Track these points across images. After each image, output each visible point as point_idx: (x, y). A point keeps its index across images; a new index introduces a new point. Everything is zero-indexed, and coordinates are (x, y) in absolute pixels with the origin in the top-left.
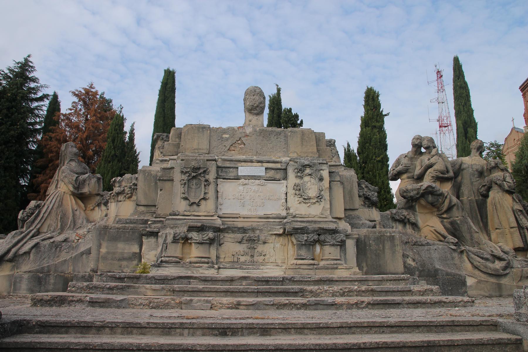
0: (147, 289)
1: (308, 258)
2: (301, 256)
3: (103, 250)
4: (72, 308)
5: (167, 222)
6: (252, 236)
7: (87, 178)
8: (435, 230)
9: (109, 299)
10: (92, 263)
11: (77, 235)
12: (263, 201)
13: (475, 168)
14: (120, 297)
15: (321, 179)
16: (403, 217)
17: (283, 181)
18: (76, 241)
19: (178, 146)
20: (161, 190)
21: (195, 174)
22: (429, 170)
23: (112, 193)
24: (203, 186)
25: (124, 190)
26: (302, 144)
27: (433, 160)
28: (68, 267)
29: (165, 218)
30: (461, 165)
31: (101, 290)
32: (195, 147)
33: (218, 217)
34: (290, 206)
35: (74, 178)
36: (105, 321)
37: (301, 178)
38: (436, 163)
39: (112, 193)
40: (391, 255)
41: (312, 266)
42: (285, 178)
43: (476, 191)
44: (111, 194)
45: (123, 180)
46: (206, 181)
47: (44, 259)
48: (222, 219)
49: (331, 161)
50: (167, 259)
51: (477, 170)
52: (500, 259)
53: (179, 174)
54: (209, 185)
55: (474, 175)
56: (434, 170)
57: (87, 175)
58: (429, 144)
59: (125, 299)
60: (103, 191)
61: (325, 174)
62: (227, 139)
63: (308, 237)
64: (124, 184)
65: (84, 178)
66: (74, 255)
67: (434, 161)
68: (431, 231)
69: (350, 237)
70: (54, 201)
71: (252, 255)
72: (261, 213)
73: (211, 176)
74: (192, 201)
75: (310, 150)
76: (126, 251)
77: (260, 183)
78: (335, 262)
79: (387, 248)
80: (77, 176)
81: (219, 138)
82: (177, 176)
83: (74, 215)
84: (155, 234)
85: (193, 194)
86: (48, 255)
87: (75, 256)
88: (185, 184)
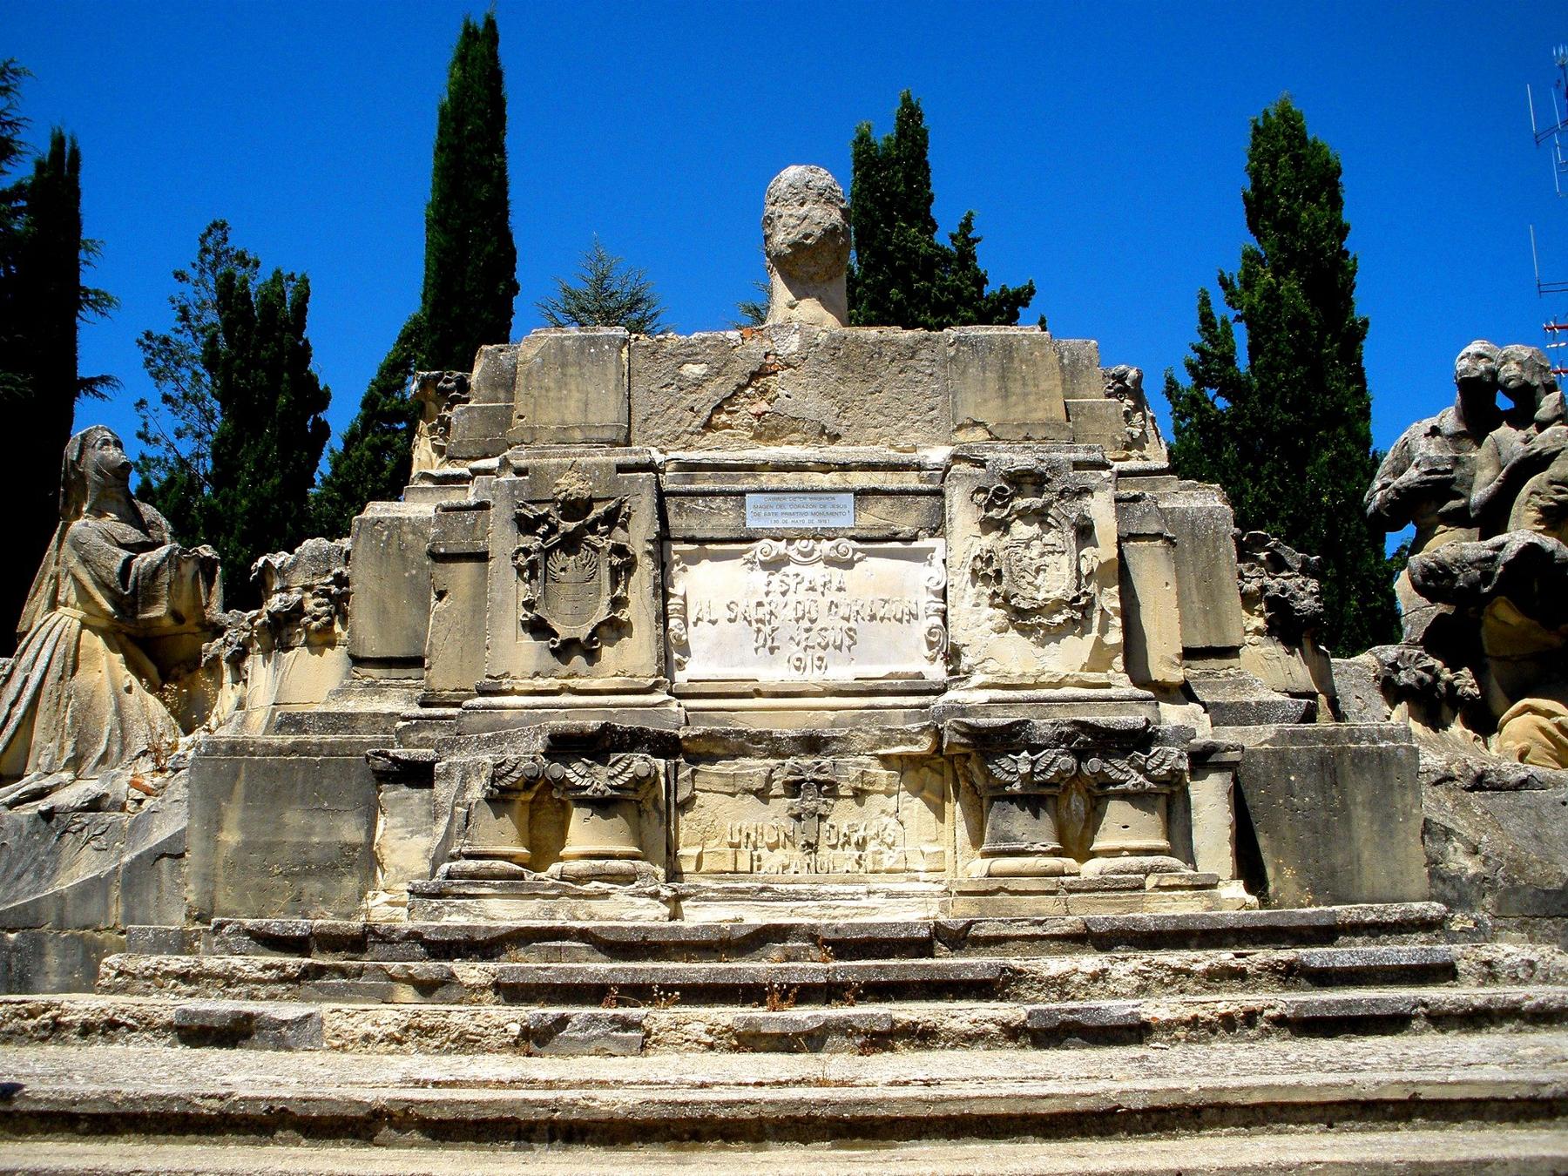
0: (393, 978)
1: (1037, 847)
2: (1006, 838)
3: (231, 837)
4: (116, 1048)
5: (466, 719)
6: (809, 768)
7: (163, 560)
8: (1560, 726)
9: (249, 1017)
10: (191, 887)
11: (133, 784)
12: (852, 624)
14: (290, 1011)
15: (1085, 532)
16: (1428, 677)
17: (925, 543)
18: (131, 806)
19: (502, 419)
20: (441, 595)
21: (571, 526)
22: (1532, 483)
23: (259, 616)
24: (605, 573)
25: (300, 603)
26: (1005, 393)
28: (107, 906)
29: (458, 705)
31: (220, 983)
32: (572, 415)
33: (670, 693)
34: (960, 642)
35: (117, 565)
36: (230, 1095)
37: (1003, 526)
38: (1556, 453)
39: (259, 616)
40: (1375, 828)
41: (1054, 879)
42: (937, 527)
44: (251, 621)
45: (294, 565)
46: (620, 550)
47: (19, 877)
48: (684, 702)
49: (1127, 458)
50: (472, 865)
53: (511, 531)
54: (630, 567)
56: (1551, 483)
57: (162, 551)
58: (1526, 376)
59: (310, 1016)
60: (226, 610)
61: (1101, 509)
62: (698, 384)
63: (1034, 763)
64: (299, 579)
65: (151, 564)
66: (126, 859)
67: (1549, 443)
68: (1542, 730)
69: (1213, 759)
70: (46, 653)
71: (809, 845)
72: (843, 672)
73: (639, 534)
74: (564, 631)
75: (1039, 415)
76: (316, 839)
77: (833, 554)
78: (1148, 861)
79: (1359, 799)
80: (124, 554)
81: (667, 380)
82: (502, 540)
83: (119, 711)
84: (418, 775)
85: (565, 606)
86: (35, 859)
87: (131, 866)
88: (533, 566)
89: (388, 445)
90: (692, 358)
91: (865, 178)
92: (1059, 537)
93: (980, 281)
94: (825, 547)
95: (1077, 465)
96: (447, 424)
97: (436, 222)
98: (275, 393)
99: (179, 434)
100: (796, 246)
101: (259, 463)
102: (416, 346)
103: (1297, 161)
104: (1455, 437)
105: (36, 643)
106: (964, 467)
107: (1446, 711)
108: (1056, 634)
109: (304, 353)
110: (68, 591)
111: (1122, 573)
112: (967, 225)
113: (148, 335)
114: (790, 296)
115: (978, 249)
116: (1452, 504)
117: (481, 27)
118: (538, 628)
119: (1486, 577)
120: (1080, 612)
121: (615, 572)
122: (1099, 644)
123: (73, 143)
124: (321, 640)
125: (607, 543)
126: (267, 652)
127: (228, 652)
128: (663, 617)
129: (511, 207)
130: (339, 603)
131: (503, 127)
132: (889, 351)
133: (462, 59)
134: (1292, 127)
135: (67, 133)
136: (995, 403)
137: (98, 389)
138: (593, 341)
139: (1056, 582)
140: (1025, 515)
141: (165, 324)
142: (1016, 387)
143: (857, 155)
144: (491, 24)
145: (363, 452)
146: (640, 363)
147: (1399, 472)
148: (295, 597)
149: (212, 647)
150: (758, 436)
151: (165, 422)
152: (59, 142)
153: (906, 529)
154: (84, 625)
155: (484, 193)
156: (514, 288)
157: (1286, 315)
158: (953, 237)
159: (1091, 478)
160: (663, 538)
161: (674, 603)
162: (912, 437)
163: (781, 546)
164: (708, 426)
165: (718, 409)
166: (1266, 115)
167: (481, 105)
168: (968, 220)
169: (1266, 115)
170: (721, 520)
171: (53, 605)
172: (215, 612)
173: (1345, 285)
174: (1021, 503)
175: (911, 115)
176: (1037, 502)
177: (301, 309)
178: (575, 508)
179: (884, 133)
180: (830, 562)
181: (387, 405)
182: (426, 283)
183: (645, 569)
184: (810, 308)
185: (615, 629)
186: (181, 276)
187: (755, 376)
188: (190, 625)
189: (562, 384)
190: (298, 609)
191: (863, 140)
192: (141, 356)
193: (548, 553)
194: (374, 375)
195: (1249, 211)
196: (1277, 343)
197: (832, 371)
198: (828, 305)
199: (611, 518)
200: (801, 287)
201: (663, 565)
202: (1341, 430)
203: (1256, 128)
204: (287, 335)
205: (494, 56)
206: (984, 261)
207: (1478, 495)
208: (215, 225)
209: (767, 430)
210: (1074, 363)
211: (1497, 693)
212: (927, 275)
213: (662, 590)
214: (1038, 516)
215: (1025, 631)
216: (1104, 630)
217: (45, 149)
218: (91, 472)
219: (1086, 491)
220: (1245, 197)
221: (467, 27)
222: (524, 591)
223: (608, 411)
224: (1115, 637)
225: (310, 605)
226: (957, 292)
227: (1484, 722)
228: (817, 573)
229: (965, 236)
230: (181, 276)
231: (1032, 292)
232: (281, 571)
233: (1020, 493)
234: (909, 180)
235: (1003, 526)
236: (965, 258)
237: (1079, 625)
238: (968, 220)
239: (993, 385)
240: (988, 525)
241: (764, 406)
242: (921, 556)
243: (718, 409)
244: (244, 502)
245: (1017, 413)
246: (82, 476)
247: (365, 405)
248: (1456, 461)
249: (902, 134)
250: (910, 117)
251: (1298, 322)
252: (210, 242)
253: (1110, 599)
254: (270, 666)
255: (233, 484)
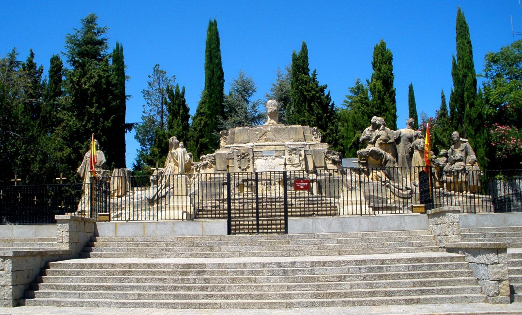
13: (408, 135)
15: (300, 155)
17: (283, 156)
19: (233, 139)
22: (378, 139)
26: (296, 134)
27: (379, 134)
30: (400, 135)
32: (242, 139)
37: (291, 155)
42: (284, 155)
43: (407, 150)
46: (248, 159)
51: (408, 138)
52: (407, 189)
53: (236, 156)
54: (250, 160)
55: (406, 140)
58: (379, 123)
61: (302, 153)
62: (258, 134)
64: (207, 159)
74: (243, 168)
75: (300, 137)
82: (236, 158)
85: (243, 165)
88: (239, 161)
89: (202, 119)
90: (257, 131)
91: (294, 62)
92: (298, 156)
93: (317, 84)
94: (272, 157)
95: (300, 147)
96: (226, 139)
97: (207, 68)
98: (179, 110)
99: (151, 111)
100: (270, 113)
101: (178, 124)
102: (206, 98)
103: (383, 56)
104: (371, 131)
105: (169, 167)
106: (287, 148)
107: (362, 172)
108: (297, 167)
109: (184, 101)
110: (172, 160)
111: (306, 159)
112: (315, 72)
113: (144, 90)
114: (270, 119)
115: (317, 77)
116: (370, 141)
117: (213, 22)
118: (240, 167)
119: (368, 154)
120: (300, 165)
121: (248, 161)
122: (302, 168)
123: (121, 45)
124: (211, 167)
125: (247, 158)
126: (203, 169)
127: (195, 168)
128: (254, 166)
129: (222, 63)
130: (214, 162)
131: (219, 45)
132: (281, 129)
133: (209, 29)
134: (383, 47)
135: (120, 43)
136: (295, 136)
137: (127, 98)
138: (244, 129)
139: (297, 161)
140: (294, 153)
141: (146, 87)
142: (297, 134)
143: (293, 58)
144: (215, 21)
145: (197, 120)
146: (250, 131)
147: (364, 136)
148: (207, 162)
149: (192, 167)
150: (265, 141)
151: (148, 108)
152: (118, 45)
153: (281, 155)
154: (175, 165)
155: (217, 61)
156: (224, 81)
157: (377, 90)
158: (312, 74)
159: (302, 149)
160: (254, 157)
161: (255, 164)
162: (284, 140)
163: (267, 157)
164: (259, 140)
165: (260, 138)
166: (377, 45)
167: (215, 41)
168: (315, 70)
169: (377, 45)
170: (260, 154)
171: (170, 162)
172: (192, 162)
173: (391, 82)
174: (293, 152)
175: (304, 46)
176: (295, 152)
177: (183, 93)
178: (243, 154)
179: (298, 51)
180: (272, 159)
181: (202, 111)
182: (206, 82)
183: (252, 160)
184: (273, 121)
185: (248, 167)
186: (149, 77)
187: (265, 133)
188: (189, 164)
189: (240, 135)
190: (208, 163)
191: (294, 54)
192: (142, 95)
193: (241, 159)
194: (198, 104)
195: (373, 66)
196: (375, 95)
197: (274, 132)
198: (275, 120)
199: (247, 155)
200: (272, 118)
201: (253, 160)
202: (388, 112)
203: (375, 48)
204: (181, 98)
205: (217, 29)
206: (318, 79)
207: (373, 140)
208: (156, 65)
209: (267, 140)
210: (306, 129)
211: (370, 169)
212: (306, 84)
213: (253, 163)
214: (295, 154)
215: (294, 167)
216: (303, 166)
217: (115, 47)
218: (174, 143)
219: (301, 150)
220: (372, 63)
221: (210, 22)
222: (238, 163)
223: (246, 138)
224: (304, 167)
225: (209, 163)
226: (312, 87)
227: (368, 174)
228: (271, 160)
229: (314, 75)
230: (149, 77)
231: (327, 86)
232: (205, 158)
233: (293, 151)
234: (304, 61)
235: (291, 155)
236: (314, 79)
237: (300, 166)
238: (315, 70)
239: (295, 134)
240: (290, 155)
241: (266, 137)
242: (282, 158)
243: (260, 138)
244: (176, 132)
245: (297, 137)
246: (172, 144)
247: (197, 111)
248: (371, 135)
249: (303, 51)
250: (304, 46)
251: (379, 92)
252: (156, 69)
253: (303, 163)
254: (204, 170)
255: (173, 128)
